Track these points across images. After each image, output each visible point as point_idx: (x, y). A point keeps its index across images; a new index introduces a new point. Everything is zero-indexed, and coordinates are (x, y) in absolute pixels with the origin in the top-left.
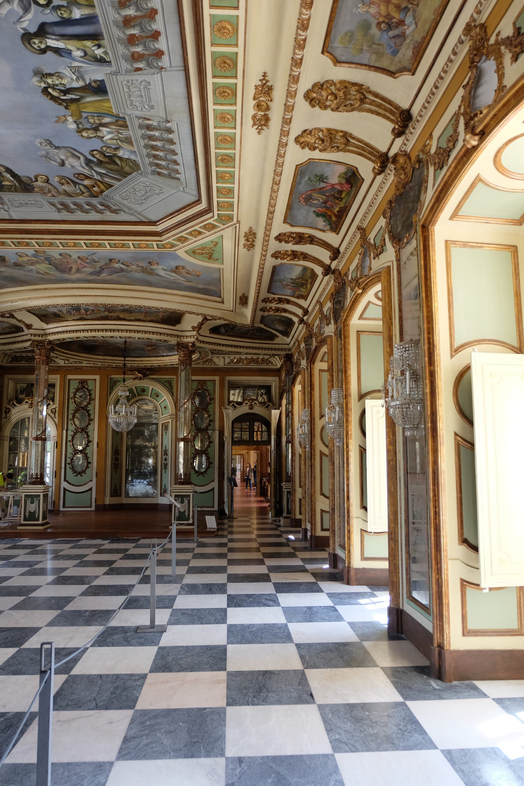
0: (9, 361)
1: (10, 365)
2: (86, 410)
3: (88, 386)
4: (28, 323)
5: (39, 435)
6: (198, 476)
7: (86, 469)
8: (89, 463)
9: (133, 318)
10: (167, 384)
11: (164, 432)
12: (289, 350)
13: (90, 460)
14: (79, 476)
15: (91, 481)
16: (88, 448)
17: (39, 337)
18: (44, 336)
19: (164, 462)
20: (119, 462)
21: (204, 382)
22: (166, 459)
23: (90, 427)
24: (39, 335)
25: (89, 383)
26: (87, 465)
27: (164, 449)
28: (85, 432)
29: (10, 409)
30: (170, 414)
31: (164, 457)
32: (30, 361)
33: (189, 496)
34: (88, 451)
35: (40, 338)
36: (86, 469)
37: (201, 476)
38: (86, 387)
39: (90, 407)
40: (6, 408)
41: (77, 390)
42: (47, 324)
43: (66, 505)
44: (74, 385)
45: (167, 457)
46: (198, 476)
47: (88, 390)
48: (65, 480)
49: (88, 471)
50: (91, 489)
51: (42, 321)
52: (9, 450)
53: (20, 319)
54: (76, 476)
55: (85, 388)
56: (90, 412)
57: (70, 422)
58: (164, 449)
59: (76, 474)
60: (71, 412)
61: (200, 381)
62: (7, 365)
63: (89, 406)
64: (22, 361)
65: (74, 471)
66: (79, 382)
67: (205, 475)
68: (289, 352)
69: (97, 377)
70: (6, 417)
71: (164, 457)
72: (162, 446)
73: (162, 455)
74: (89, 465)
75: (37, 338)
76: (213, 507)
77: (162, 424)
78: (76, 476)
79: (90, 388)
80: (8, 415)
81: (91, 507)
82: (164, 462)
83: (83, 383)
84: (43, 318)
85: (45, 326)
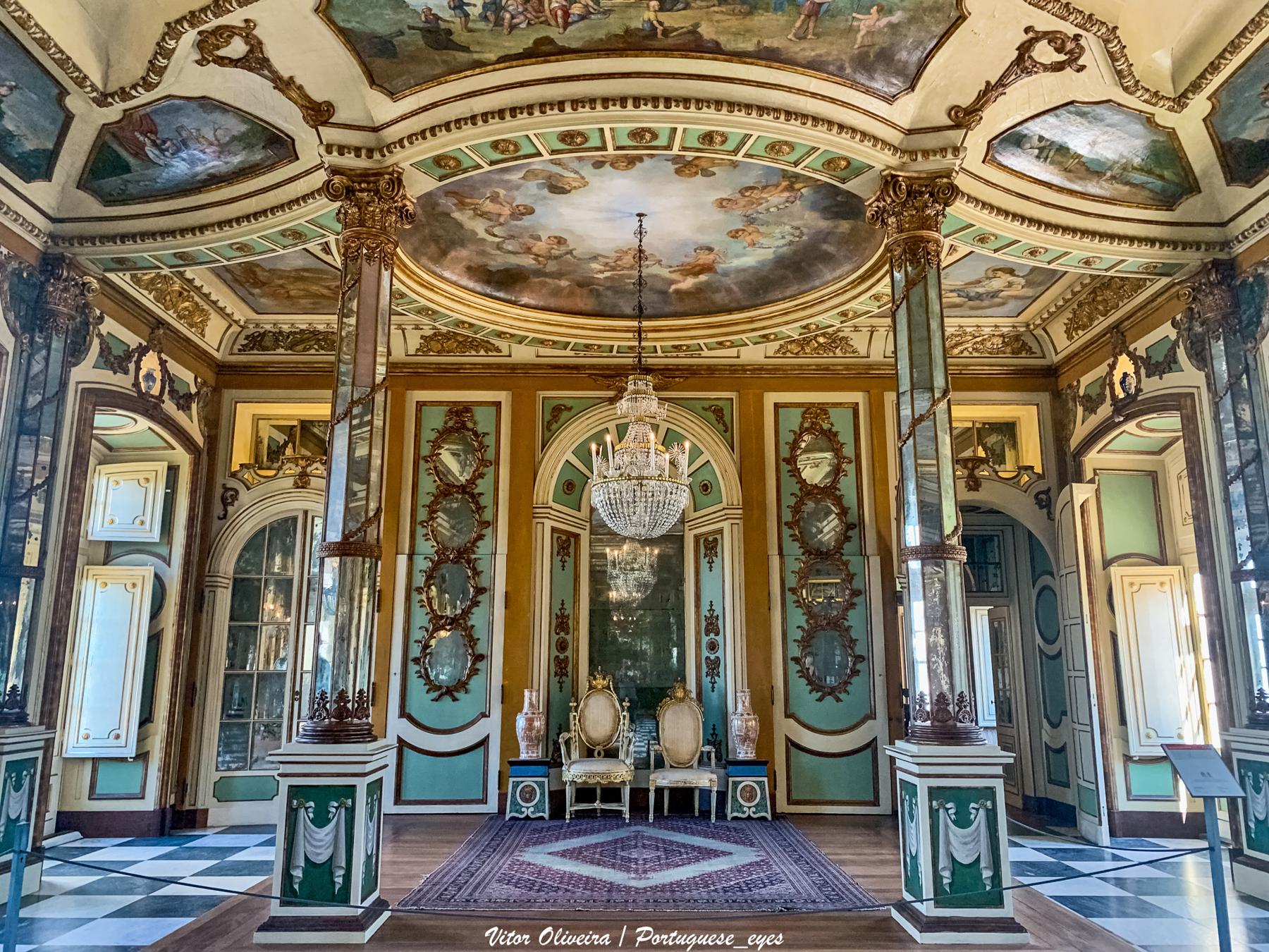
0: (237, 347)
1: (243, 358)
2: (473, 496)
3: (475, 423)
4: (318, 96)
5: (352, 534)
6: (820, 700)
7: (469, 676)
8: (479, 658)
9: (749, 46)
10: (711, 415)
11: (704, 562)
12: (1225, 244)
13: (481, 648)
14: (447, 699)
15: (484, 715)
16: (475, 610)
17: (358, 156)
18: (377, 156)
19: (705, 653)
20: (569, 653)
21: (823, 409)
22: (713, 647)
23: (483, 548)
24: (357, 151)
25: (479, 413)
26: (473, 664)
27: (705, 611)
28: (469, 562)
29: (237, 492)
30: (724, 504)
31: (705, 639)
32: (300, 347)
33: (990, 793)
34: (477, 619)
35: (362, 163)
36: (469, 676)
37: (829, 699)
38: (470, 425)
39: (483, 486)
40: (226, 489)
41: (444, 435)
42: (392, 95)
43: (406, 796)
44: (435, 420)
45: (720, 639)
46: (820, 700)
47: (476, 434)
48: (404, 714)
49: (475, 683)
50: (484, 743)
51: (372, 82)
52: (232, 619)
53: (285, 74)
54: (436, 700)
55: (468, 430)
56: (484, 501)
57: (420, 531)
58: (705, 611)
59: (435, 694)
60: (425, 499)
61: (808, 408)
62: (234, 359)
63: (479, 481)
64: (278, 346)
65: (432, 686)
66: (450, 411)
67: (842, 696)
68: (1222, 256)
69: (503, 396)
70: (225, 516)
71: (705, 639)
72: (698, 606)
73: (698, 633)
74: (479, 665)
75: (349, 161)
76: (876, 803)
77: (697, 538)
78: (436, 700)
79: (480, 429)
80: (230, 509)
81: (484, 801)
82: (705, 653)
83: (460, 412)
84: (379, 64)
85: (382, 108)
